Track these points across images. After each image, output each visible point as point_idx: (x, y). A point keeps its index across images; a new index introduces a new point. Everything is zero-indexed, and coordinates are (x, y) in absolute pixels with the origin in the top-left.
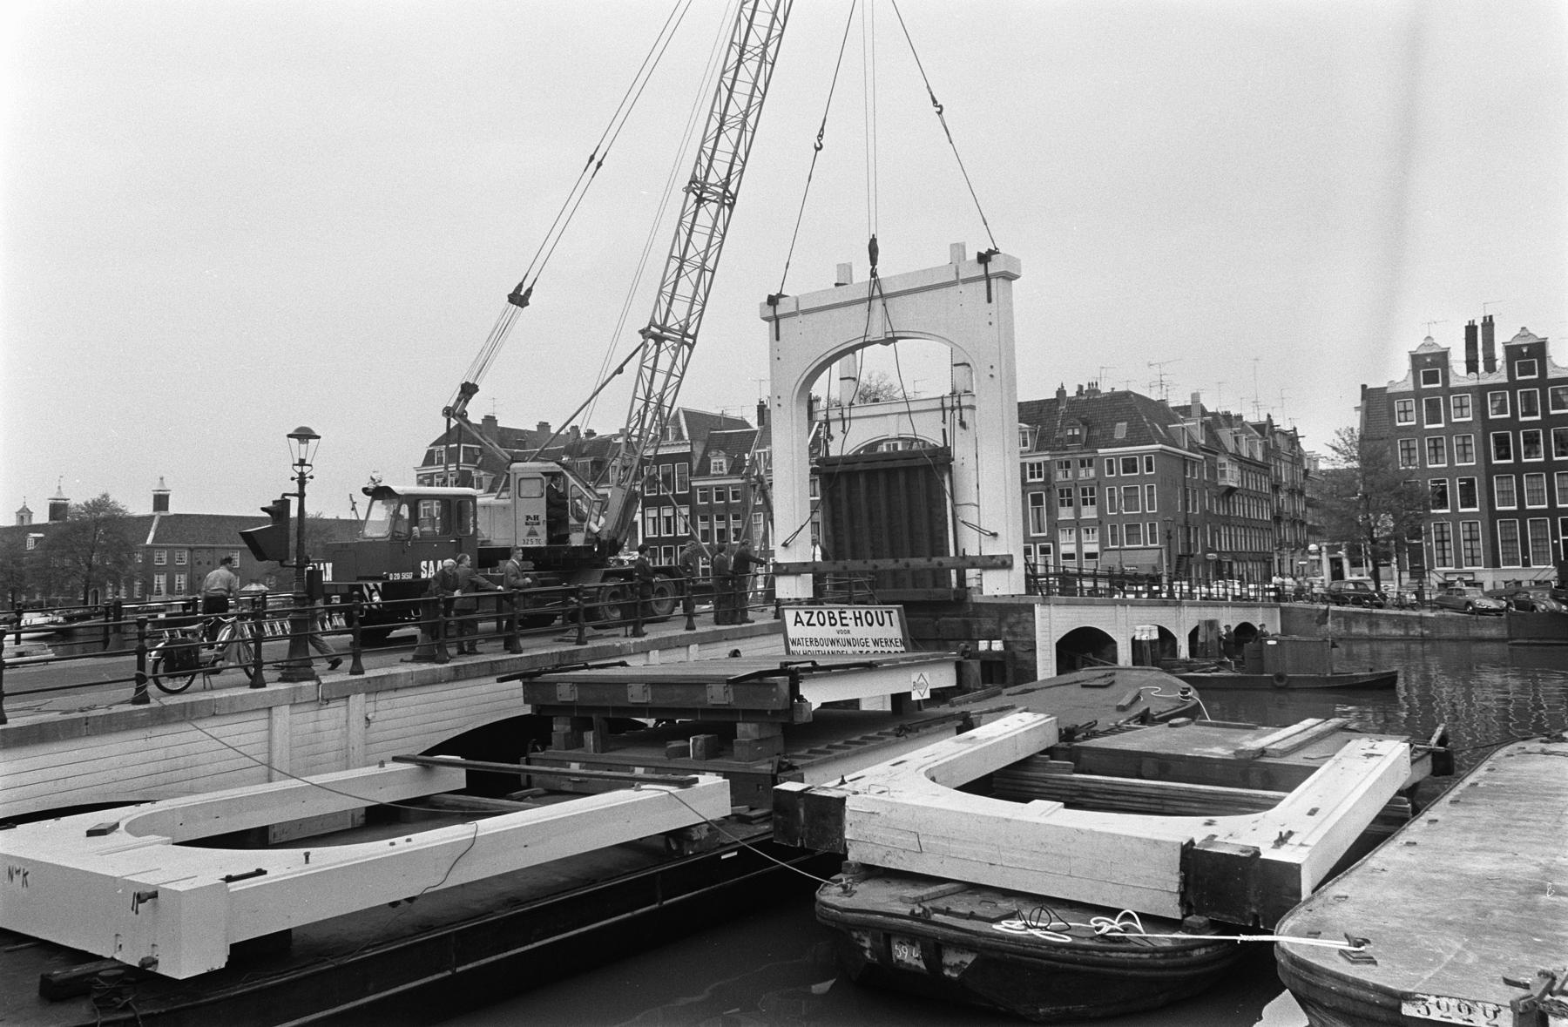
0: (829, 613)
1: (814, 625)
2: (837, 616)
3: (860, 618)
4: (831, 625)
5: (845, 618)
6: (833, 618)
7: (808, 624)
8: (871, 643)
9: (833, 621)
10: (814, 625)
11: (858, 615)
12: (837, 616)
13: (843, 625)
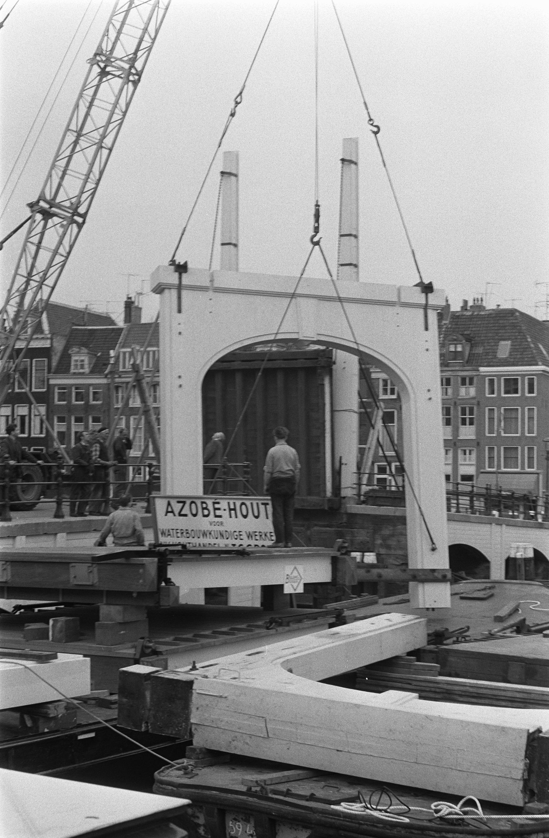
0: (203, 503)
1: (185, 515)
2: (211, 507)
3: (234, 509)
4: (205, 516)
5: (219, 509)
6: (206, 508)
7: (180, 515)
8: (244, 536)
9: (206, 512)
10: (185, 515)
11: (232, 507)
12: (211, 507)
13: (216, 516)
